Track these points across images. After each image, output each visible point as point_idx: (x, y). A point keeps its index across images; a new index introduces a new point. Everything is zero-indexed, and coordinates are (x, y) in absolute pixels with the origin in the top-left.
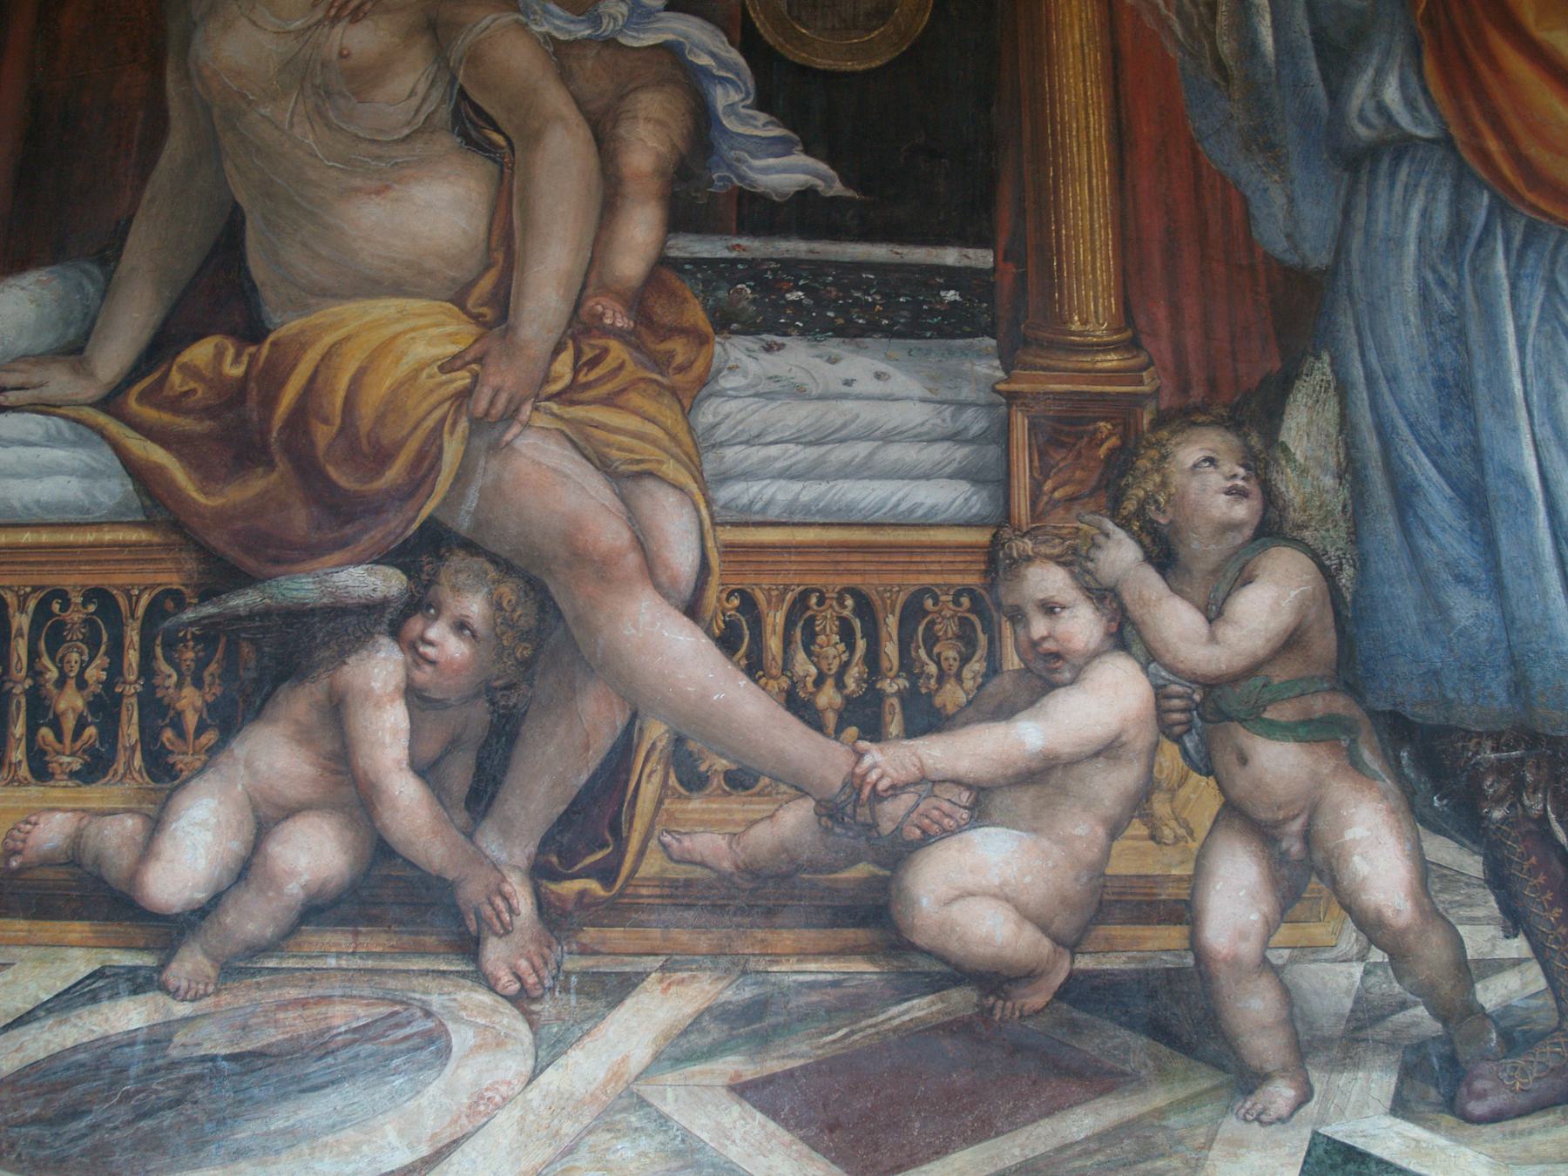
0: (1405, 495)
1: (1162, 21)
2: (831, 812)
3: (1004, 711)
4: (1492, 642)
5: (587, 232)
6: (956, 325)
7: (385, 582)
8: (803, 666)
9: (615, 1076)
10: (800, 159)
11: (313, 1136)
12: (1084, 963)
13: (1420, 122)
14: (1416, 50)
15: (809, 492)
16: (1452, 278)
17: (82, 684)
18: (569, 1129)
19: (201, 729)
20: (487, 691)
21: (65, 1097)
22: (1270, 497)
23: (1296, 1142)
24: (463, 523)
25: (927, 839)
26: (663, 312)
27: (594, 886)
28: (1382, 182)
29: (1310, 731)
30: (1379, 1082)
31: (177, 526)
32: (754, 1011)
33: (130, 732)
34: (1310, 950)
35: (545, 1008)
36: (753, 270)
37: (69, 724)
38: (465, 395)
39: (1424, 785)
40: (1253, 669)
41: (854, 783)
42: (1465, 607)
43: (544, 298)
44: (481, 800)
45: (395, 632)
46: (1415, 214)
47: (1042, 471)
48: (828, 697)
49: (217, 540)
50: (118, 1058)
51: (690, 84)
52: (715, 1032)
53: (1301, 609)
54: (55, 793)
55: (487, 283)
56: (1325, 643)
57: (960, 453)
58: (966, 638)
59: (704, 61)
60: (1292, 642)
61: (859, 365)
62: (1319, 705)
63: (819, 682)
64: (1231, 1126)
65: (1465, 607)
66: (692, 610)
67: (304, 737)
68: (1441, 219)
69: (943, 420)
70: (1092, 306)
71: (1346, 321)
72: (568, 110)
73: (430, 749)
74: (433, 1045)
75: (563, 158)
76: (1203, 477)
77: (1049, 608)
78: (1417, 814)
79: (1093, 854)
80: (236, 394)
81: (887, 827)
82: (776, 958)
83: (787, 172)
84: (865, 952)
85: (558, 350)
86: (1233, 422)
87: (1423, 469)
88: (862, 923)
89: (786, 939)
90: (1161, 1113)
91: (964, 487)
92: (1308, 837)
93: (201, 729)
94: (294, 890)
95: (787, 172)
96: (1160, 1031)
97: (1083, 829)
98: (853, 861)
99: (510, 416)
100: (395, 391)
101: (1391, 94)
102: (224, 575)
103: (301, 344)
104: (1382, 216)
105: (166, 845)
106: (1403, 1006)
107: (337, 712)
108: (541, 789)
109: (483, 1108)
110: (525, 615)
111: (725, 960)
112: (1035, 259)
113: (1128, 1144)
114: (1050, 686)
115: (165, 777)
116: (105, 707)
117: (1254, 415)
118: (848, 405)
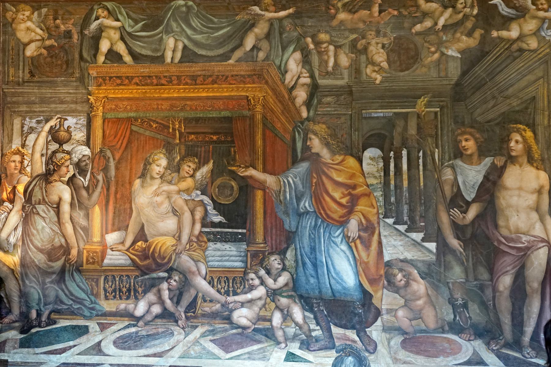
0: (304, 264)
1: (272, 194)
2: (223, 305)
4: (316, 285)
5: (191, 228)
6: (241, 240)
7: (165, 275)
8: (219, 286)
9: (195, 338)
10: (219, 217)
11: (156, 345)
12: (256, 326)
13: (311, 209)
14: (311, 198)
15: (220, 263)
16: (314, 232)
17: (126, 287)
18: (189, 345)
19: (142, 293)
20: (178, 289)
21: (125, 340)
22: (284, 264)
23: (285, 352)
24: (175, 267)
25: (235, 309)
26: (201, 239)
27: (192, 314)
28: (304, 218)
29: (289, 297)
31: (137, 267)
33: (132, 293)
35: (186, 329)
36: (213, 233)
37: (124, 292)
38: (175, 250)
39: (305, 304)
40: (281, 288)
41: (226, 302)
42: (312, 280)
43: (185, 238)
44: (178, 303)
45: (167, 281)
46: (309, 223)
47: (252, 261)
48: (223, 291)
49: (143, 269)
50: (132, 335)
52: (208, 333)
53: (288, 280)
54: (122, 301)
55: (177, 235)
56: (291, 285)
57: (241, 258)
58: (241, 283)
59: (206, 202)
60: (286, 285)
61: (227, 246)
62: (290, 293)
63: (221, 288)
64: (276, 349)
65: (312, 280)
66: (205, 279)
67: (155, 295)
68: (313, 223)
69: (238, 254)
70: (260, 238)
71: (297, 239)
72: (188, 210)
73: (171, 296)
74: (172, 334)
75: (187, 216)
76: (275, 262)
77: (252, 279)
78: (303, 309)
79: (258, 312)
80: (144, 249)
81: (230, 308)
82: (216, 324)
83: (218, 219)
84: (227, 324)
85: (187, 244)
86: (279, 254)
87: (307, 261)
88: (227, 320)
89: (217, 322)
90: (266, 347)
91: (241, 263)
92: (288, 311)
93: (142, 293)
94: (154, 314)
95: (218, 219)
96: (266, 336)
97: (256, 309)
98: (226, 312)
99: (181, 253)
100: (165, 249)
101: (307, 205)
103: (153, 242)
104: (304, 223)
105: (137, 308)
106: (301, 335)
107: (159, 291)
108: (186, 301)
109: (178, 342)
110: (183, 279)
112: (252, 231)
113: (262, 351)
114: (252, 290)
118: (226, 252)
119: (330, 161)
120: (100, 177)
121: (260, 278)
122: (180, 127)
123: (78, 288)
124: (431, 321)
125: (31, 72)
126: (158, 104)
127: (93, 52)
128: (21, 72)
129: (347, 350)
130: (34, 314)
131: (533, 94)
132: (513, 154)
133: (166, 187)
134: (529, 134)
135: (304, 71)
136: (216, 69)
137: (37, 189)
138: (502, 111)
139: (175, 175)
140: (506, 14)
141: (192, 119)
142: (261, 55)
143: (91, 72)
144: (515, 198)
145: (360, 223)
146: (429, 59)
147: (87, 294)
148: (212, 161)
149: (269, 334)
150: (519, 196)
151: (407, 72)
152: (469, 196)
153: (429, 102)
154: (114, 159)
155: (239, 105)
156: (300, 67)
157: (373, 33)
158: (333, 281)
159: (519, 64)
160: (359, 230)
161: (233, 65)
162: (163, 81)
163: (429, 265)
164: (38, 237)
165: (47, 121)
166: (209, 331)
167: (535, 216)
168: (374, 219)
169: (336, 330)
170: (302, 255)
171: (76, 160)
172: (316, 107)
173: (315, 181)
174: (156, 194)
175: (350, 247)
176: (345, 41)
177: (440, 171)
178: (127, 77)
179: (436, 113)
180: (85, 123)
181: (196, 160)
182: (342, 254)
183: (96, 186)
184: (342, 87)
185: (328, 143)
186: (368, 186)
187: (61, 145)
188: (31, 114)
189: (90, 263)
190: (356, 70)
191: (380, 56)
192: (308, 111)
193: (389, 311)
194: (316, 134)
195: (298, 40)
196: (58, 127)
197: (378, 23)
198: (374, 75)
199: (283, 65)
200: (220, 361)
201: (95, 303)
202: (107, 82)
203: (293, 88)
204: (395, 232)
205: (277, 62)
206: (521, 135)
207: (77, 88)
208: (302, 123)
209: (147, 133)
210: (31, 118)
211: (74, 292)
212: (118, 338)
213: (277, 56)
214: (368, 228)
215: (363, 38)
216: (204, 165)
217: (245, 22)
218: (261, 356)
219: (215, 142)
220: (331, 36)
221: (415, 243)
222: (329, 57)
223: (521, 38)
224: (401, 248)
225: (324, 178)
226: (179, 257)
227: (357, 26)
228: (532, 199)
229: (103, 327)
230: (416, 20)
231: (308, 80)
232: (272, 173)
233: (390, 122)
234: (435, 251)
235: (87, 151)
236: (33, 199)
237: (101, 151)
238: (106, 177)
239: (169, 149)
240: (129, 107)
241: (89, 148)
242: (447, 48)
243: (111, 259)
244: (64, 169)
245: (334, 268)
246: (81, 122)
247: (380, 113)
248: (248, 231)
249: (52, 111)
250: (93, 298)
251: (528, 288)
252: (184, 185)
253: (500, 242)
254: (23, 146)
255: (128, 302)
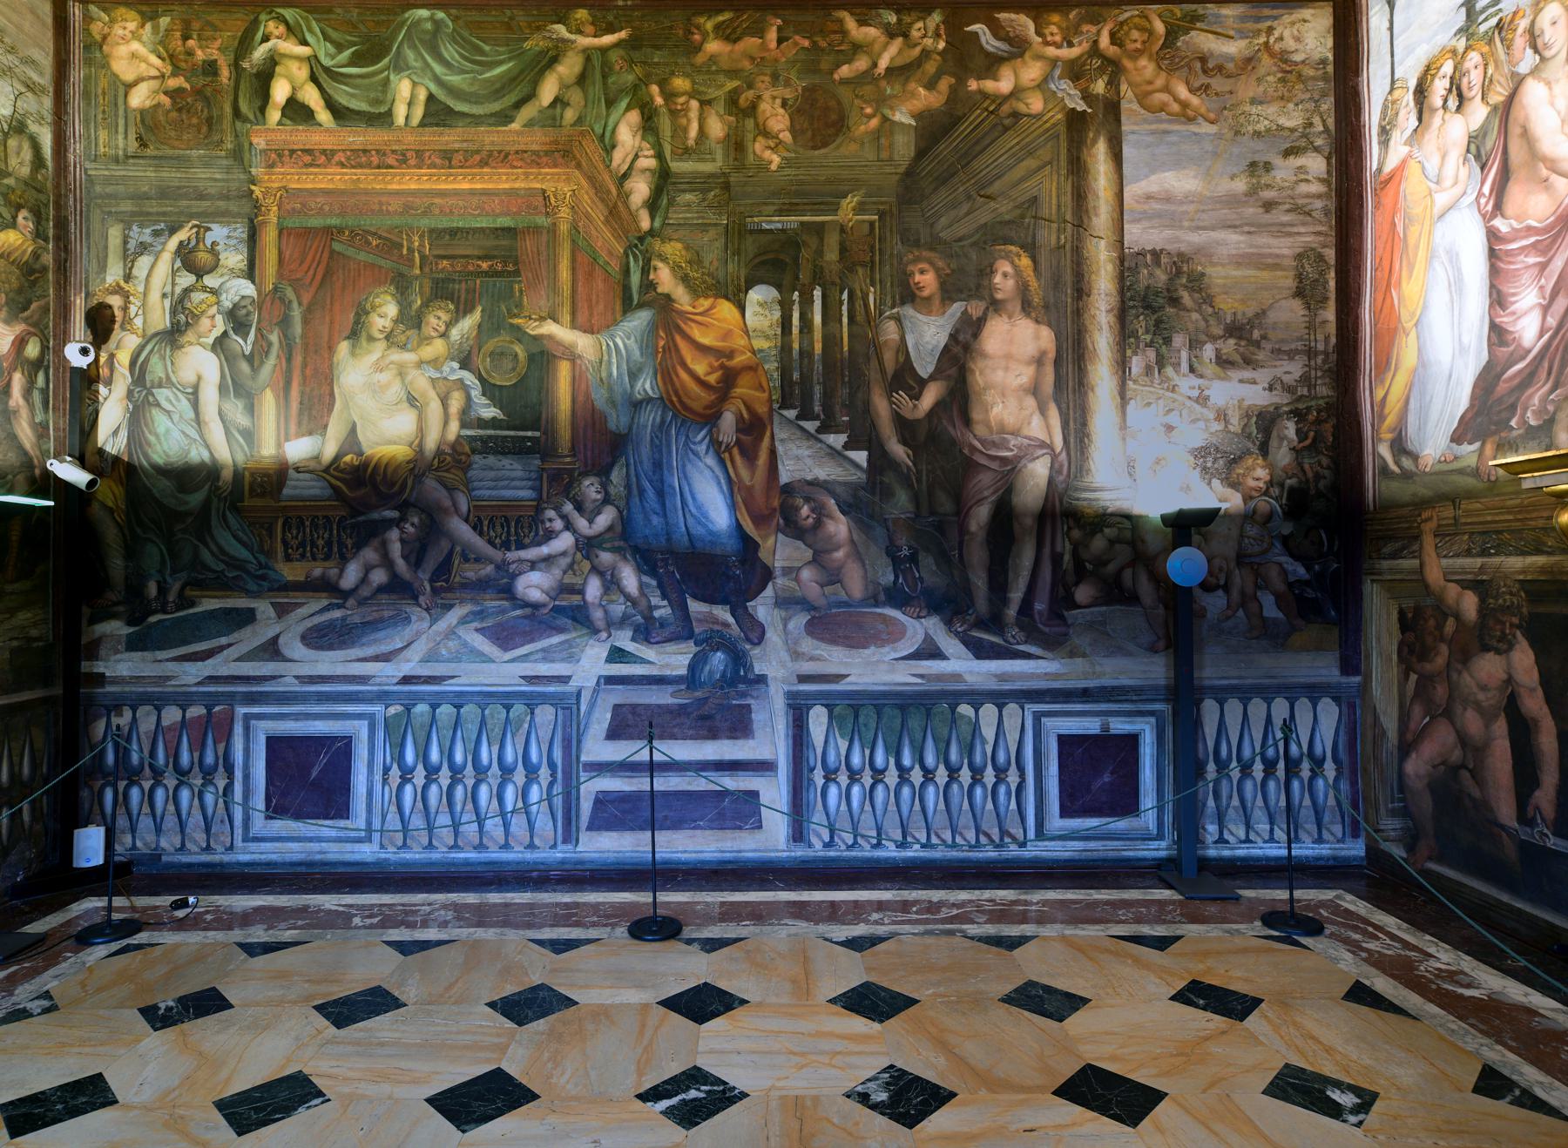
0: (642, 492)
2: (498, 567)
3: (539, 544)
7: (395, 514)
15: (494, 493)
22: (607, 493)
24: (412, 500)
29: (613, 550)
30: (629, 633)
32: (481, 612)
34: (612, 602)
40: (601, 534)
41: (504, 561)
42: (656, 520)
51: (465, 389)
56: (619, 529)
58: (530, 527)
60: (610, 528)
61: (506, 462)
65: (656, 520)
66: (466, 521)
67: (376, 550)
68: (658, 419)
69: (526, 475)
74: (408, 620)
75: (434, 407)
76: (590, 489)
78: (640, 570)
87: (647, 485)
96: (574, 619)
97: (557, 572)
101: (648, 386)
102: (355, 512)
109: (418, 635)
111: (474, 601)
115: (344, 560)
116: (329, 544)
117: (603, 472)
119: (690, 309)
120: (274, 338)
121: (564, 517)
122: (422, 245)
123: (234, 542)
124: (855, 584)
125: (140, 138)
126: (381, 203)
127: (259, 103)
128: (121, 137)
129: (714, 640)
130: (152, 589)
131: (1035, 192)
132: (999, 296)
133: (397, 356)
134: (1025, 262)
135: (646, 145)
136: (487, 139)
137: (155, 359)
138: (982, 221)
139: (412, 333)
140: (991, 49)
141: (444, 230)
142: (570, 115)
143: (255, 140)
144: (1000, 373)
145: (740, 419)
146: (862, 128)
147: (251, 550)
148: (479, 309)
149: (579, 617)
150: (1007, 369)
151: (822, 151)
152: (925, 368)
153: (861, 204)
154: (300, 304)
155: (528, 207)
156: (638, 138)
157: (767, 79)
158: (690, 521)
159: (1011, 140)
160: (738, 431)
161: (518, 133)
162: (391, 160)
163: (854, 488)
164: (158, 447)
165: (173, 231)
166: (474, 613)
167: (1030, 402)
168: (762, 410)
169: (695, 607)
170: (637, 476)
171: (228, 304)
172: (667, 212)
173: (662, 343)
174: (379, 368)
175: (722, 462)
176: (717, 93)
177: (877, 326)
178: (324, 152)
179: (872, 224)
180: (245, 236)
181: (451, 307)
182: (707, 472)
183: (267, 353)
184: (712, 175)
185: (686, 275)
186: (753, 352)
187: (199, 276)
188: (142, 217)
189: (258, 495)
190: (736, 145)
191: (778, 121)
192: (652, 218)
193: (787, 571)
194: (664, 260)
195: (636, 87)
196: (193, 243)
197: (776, 60)
198: (767, 154)
199: (608, 134)
200: (493, 666)
201: (267, 567)
202: (286, 159)
203: (625, 176)
204: (799, 433)
205: (598, 129)
206: (1012, 263)
207: (228, 170)
208: (641, 239)
209: (362, 256)
210: (141, 226)
211: (227, 548)
212: (310, 629)
213: (598, 117)
214: (753, 427)
215: (750, 86)
216: (465, 314)
217: (540, 52)
218: (564, 654)
219: (486, 274)
220: (694, 83)
221: (834, 453)
222: (689, 120)
223: (1017, 93)
224: (809, 462)
225: (678, 339)
226: (420, 482)
227: (740, 66)
228: (1025, 375)
229: (282, 611)
230: (841, 57)
231: (651, 163)
232: (589, 330)
233: (789, 242)
234: (865, 465)
235: (248, 289)
236: (148, 378)
237: (276, 289)
238: (285, 336)
239: (401, 286)
240: (327, 208)
241: (253, 282)
242: (892, 108)
243: (295, 487)
244: (205, 322)
245: (694, 498)
246: (236, 234)
247: (775, 223)
248: (545, 433)
249: (181, 213)
250: (263, 559)
251: (1016, 527)
252: (428, 352)
253: (973, 449)
254: (128, 277)
255: (327, 564)
